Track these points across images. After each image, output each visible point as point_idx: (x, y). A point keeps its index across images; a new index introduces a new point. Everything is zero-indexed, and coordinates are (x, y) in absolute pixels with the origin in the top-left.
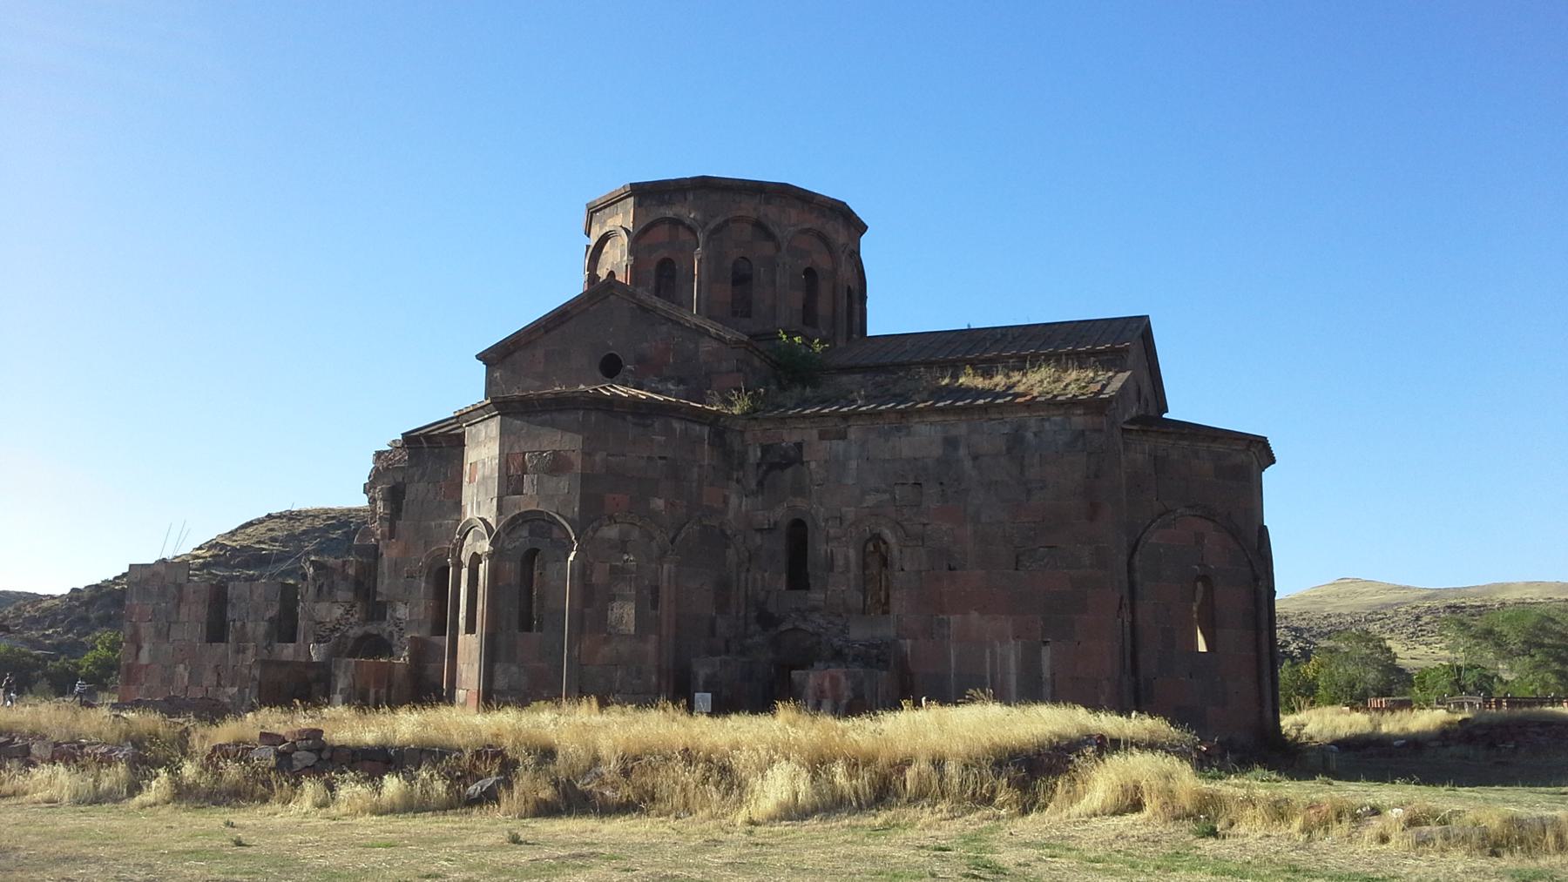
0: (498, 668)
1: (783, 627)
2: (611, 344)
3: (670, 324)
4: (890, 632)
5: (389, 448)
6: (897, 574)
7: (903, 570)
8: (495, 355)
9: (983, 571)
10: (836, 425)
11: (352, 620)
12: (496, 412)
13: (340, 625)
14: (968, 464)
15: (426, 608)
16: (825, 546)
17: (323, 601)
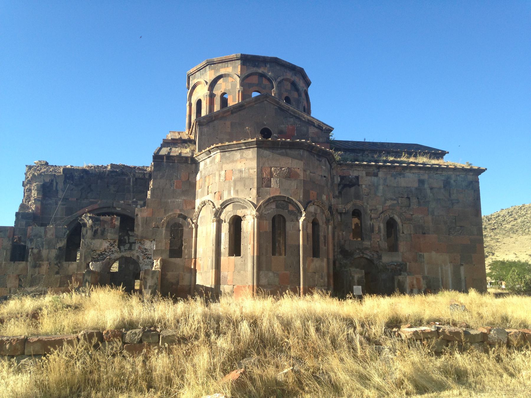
0: (261, 273)
1: (356, 256)
2: (265, 123)
3: (294, 118)
4: (400, 260)
5: (35, 165)
6: (401, 235)
7: (403, 233)
8: (205, 121)
9: (437, 235)
10: (374, 170)
11: (113, 249)
12: (256, 146)
13: (106, 252)
14: (428, 191)
15: (166, 244)
16: (370, 222)
17: (98, 238)
